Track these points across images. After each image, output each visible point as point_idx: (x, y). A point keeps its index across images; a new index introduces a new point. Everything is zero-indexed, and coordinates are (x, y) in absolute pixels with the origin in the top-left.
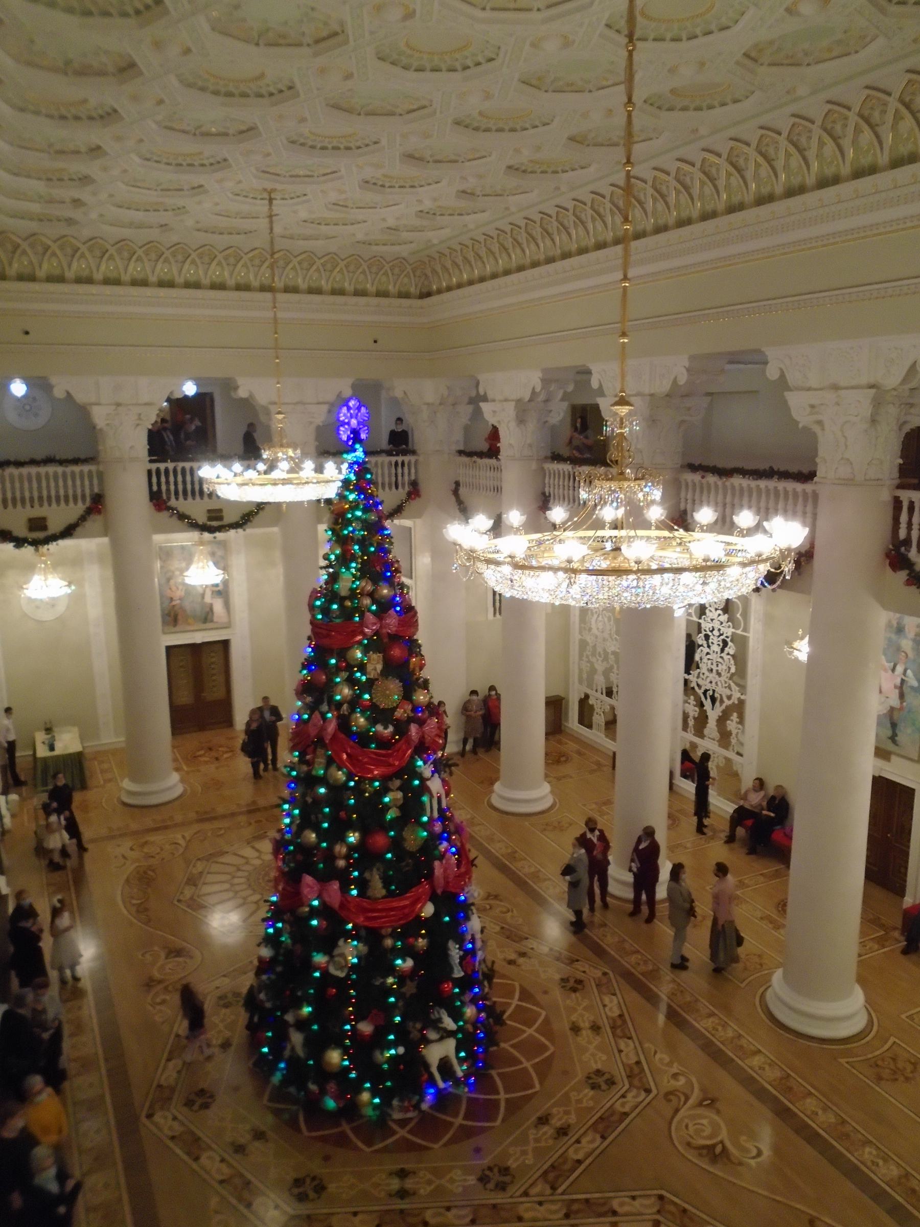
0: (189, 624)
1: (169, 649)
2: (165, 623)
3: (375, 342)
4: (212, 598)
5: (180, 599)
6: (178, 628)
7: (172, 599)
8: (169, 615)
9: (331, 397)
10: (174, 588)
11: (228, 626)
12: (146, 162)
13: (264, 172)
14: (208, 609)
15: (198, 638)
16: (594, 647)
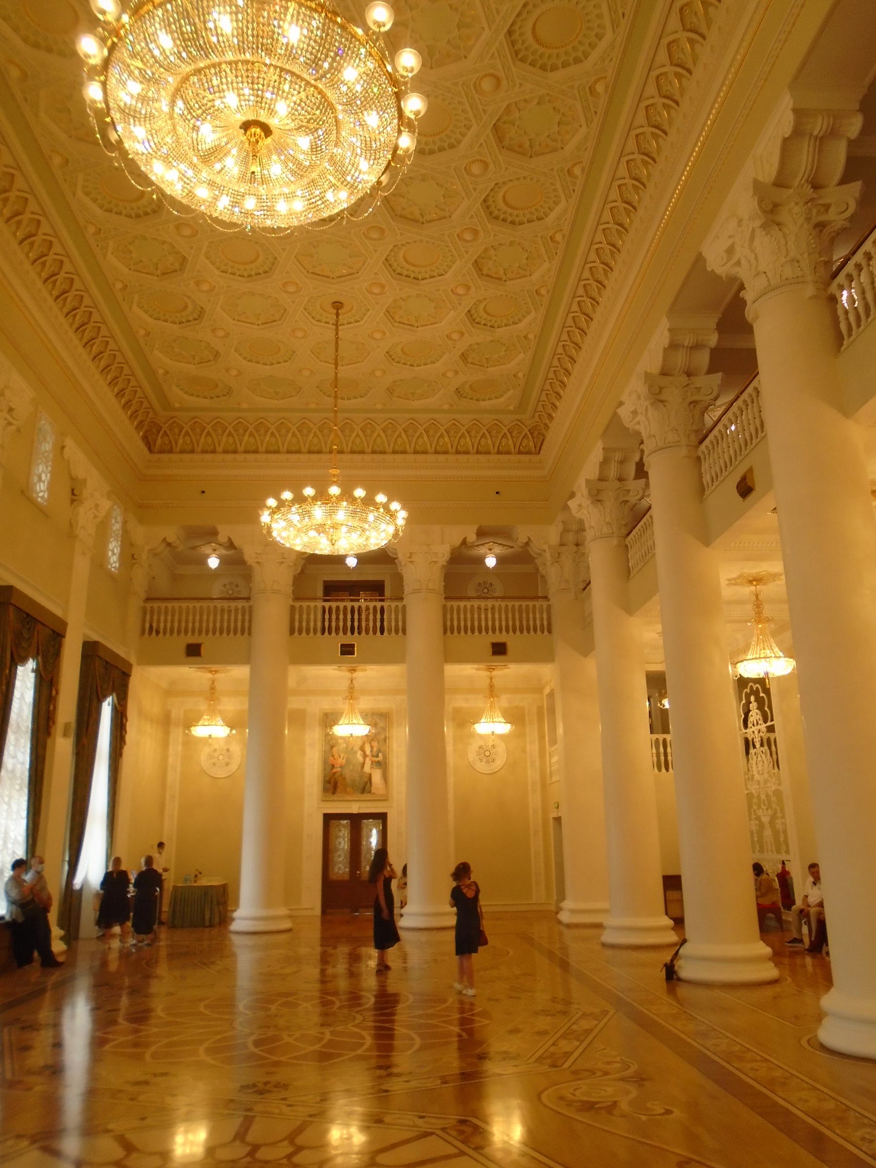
0: (347, 793)
1: (328, 818)
2: (325, 790)
3: (497, 493)
4: (371, 768)
5: (341, 767)
6: (335, 797)
7: (333, 766)
8: (329, 782)
9: (457, 542)
10: (336, 756)
11: (385, 798)
12: (222, 274)
13: (312, 273)
14: (366, 780)
15: (355, 808)
16: (759, 797)
